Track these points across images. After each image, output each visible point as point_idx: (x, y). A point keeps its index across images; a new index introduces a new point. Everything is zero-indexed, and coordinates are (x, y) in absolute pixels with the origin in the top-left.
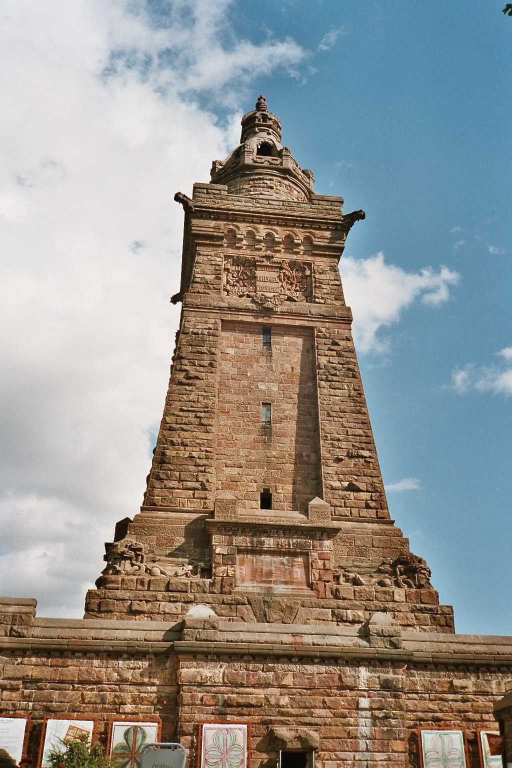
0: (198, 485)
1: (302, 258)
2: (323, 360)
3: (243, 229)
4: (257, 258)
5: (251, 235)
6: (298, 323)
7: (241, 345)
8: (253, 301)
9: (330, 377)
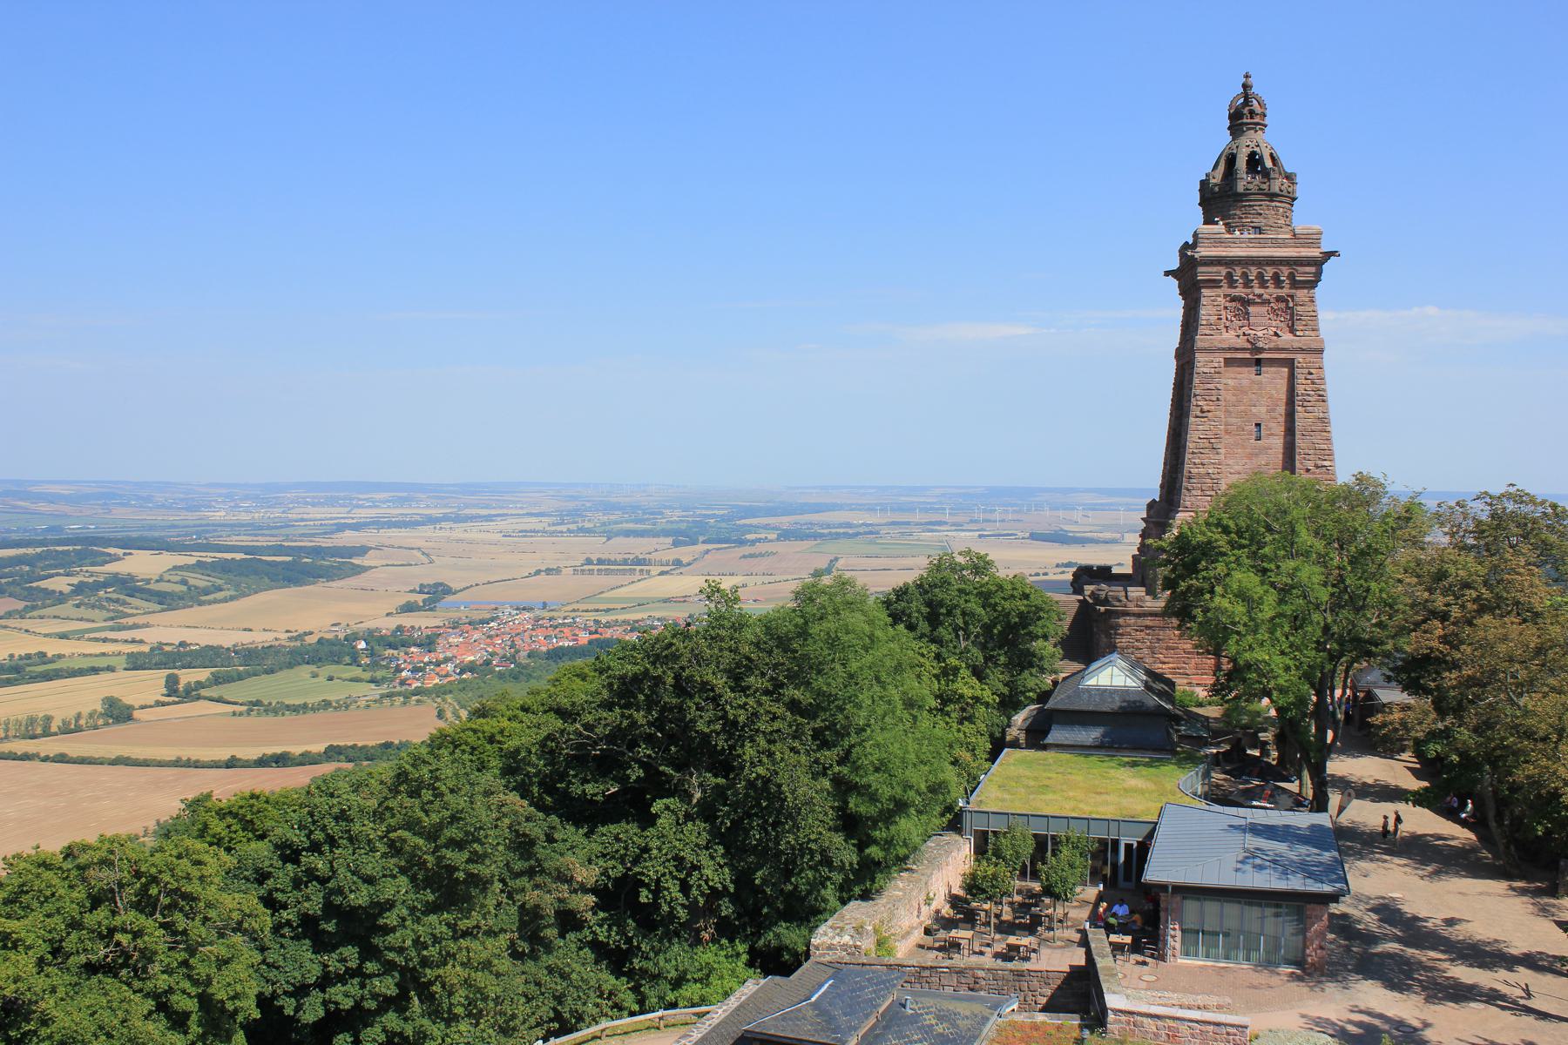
0: (1213, 493)
1: (1284, 292)
2: (1300, 389)
3: (1238, 271)
4: (1251, 297)
5: (1245, 275)
6: (1283, 356)
7: (1239, 376)
8: (1248, 341)
9: (1305, 404)
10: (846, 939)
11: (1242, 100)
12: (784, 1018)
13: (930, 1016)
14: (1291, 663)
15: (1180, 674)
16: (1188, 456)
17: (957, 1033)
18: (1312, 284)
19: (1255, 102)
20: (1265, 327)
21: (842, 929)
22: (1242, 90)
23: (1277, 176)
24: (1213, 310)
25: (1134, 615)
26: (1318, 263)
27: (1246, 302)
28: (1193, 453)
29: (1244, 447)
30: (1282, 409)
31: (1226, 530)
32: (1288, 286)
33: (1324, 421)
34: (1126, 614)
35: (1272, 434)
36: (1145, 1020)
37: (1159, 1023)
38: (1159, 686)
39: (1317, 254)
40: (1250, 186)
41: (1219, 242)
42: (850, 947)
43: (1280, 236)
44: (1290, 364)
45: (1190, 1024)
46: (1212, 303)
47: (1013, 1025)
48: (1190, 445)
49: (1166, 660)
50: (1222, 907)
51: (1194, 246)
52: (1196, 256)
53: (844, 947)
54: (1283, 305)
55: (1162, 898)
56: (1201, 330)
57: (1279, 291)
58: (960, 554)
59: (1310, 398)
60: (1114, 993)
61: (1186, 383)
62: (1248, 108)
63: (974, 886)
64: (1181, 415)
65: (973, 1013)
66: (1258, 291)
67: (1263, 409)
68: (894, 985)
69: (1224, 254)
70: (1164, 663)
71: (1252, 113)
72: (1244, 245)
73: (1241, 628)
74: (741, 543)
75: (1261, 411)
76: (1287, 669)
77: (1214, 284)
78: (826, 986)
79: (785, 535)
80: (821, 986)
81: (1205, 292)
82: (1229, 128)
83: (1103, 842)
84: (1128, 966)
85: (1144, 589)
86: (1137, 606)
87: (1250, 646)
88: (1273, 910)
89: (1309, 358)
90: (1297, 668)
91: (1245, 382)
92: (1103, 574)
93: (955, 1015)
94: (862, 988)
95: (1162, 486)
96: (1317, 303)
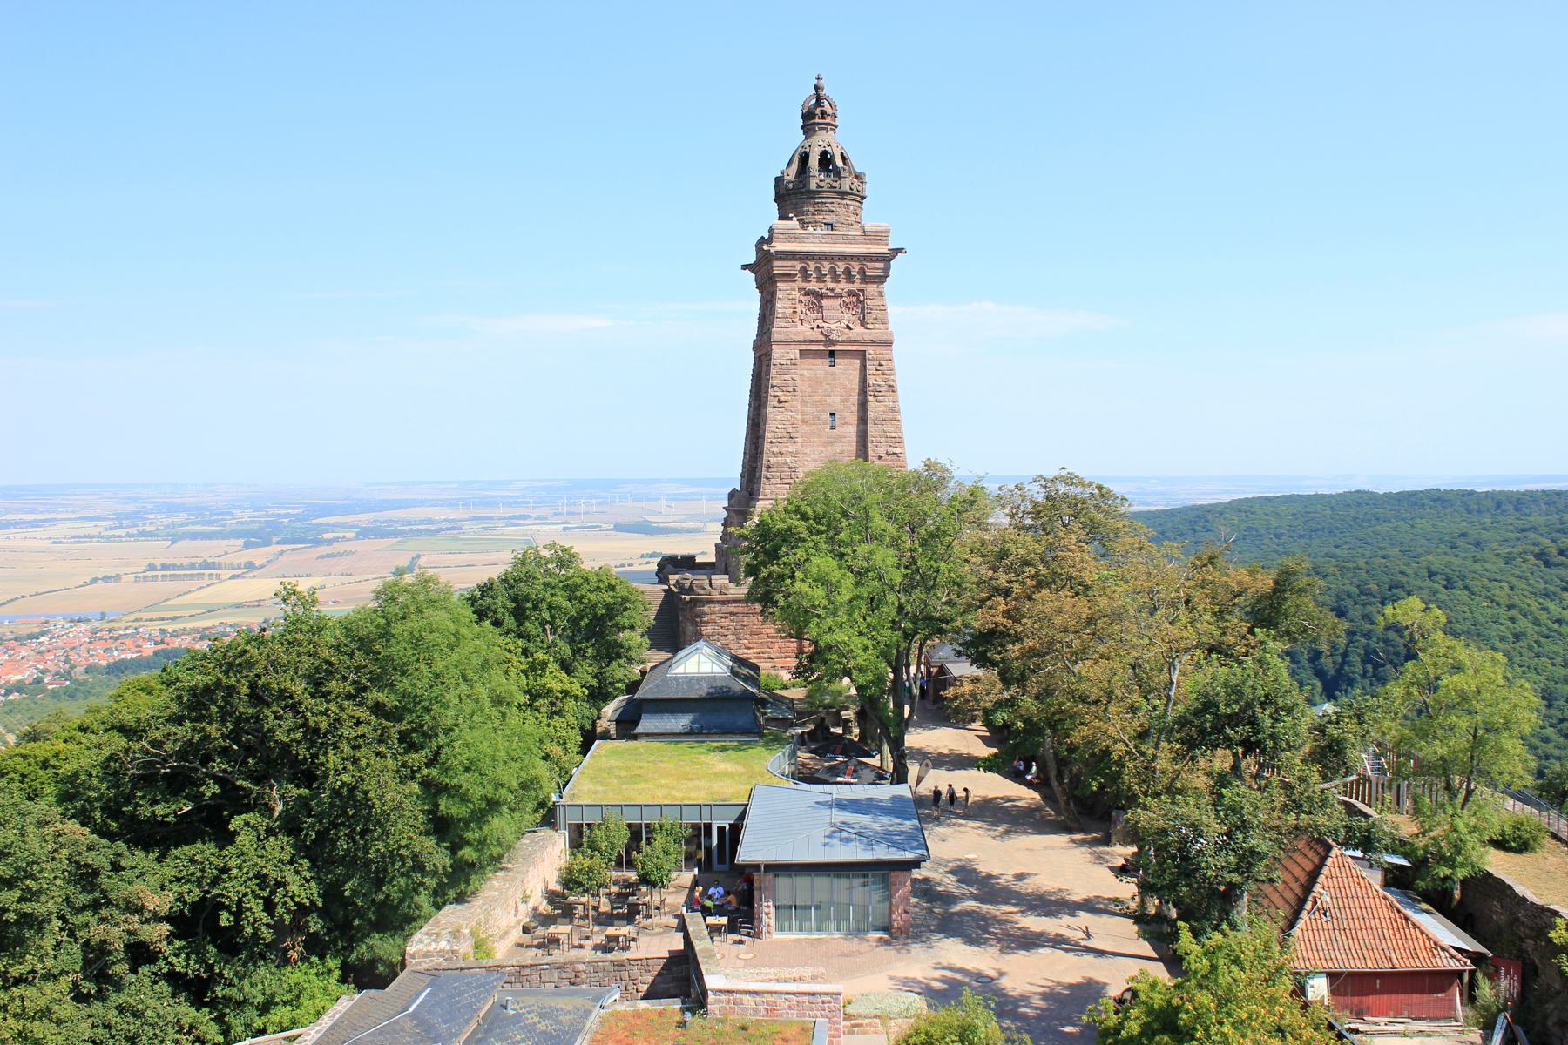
0: (792, 481)
1: (855, 287)
2: (871, 380)
3: (812, 266)
4: (824, 291)
5: (818, 270)
6: (855, 348)
9: (876, 394)
10: (443, 944)
11: (814, 101)
12: (381, 1032)
13: (532, 1015)
14: (869, 643)
15: (764, 658)
16: (766, 445)
17: (560, 1029)
18: (881, 279)
19: (826, 103)
20: (837, 319)
21: (438, 935)
22: (814, 91)
23: (847, 175)
24: (789, 304)
25: (718, 602)
26: (886, 259)
27: (820, 296)
28: (771, 443)
29: (820, 436)
30: (855, 399)
31: (804, 517)
32: (859, 281)
33: (894, 410)
34: (711, 602)
35: (846, 423)
36: (744, 997)
37: (758, 998)
38: (745, 671)
39: (886, 251)
40: (822, 184)
41: (794, 237)
42: (448, 952)
43: (851, 233)
44: (862, 355)
45: (787, 997)
46: (787, 296)
47: (615, 1015)
48: (769, 435)
49: (750, 645)
50: (812, 880)
51: (769, 241)
52: (772, 250)
53: (441, 953)
54: (854, 299)
55: (755, 878)
56: (778, 322)
57: (851, 285)
58: (545, 547)
59: (880, 389)
60: (713, 973)
61: (763, 374)
62: (819, 109)
63: (570, 881)
64: (760, 405)
65: (575, 1008)
66: (831, 285)
67: (838, 400)
68: (494, 987)
69: (798, 249)
70: (749, 648)
71: (823, 114)
72: (817, 241)
73: (821, 611)
74: (318, 542)
75: (835, 401)
76: (866, 648)
77: (789, 278)
78: (424, 994)
79: (365, 533)
80: (418, 995)
81: (780, 285)
82: (802, 128)
83: (695, 827)
84: (725, 945)
85: (727, 576)
86: (721, 593)
87: (830, 628)
88: (861, 880)
89: (881, 350)
90: (875, 647)
91: (820, 373)
92: (688, 563)
93: (557, 1011)
94: (461, 994)
95: (742, 476)
96: (886, 297)
